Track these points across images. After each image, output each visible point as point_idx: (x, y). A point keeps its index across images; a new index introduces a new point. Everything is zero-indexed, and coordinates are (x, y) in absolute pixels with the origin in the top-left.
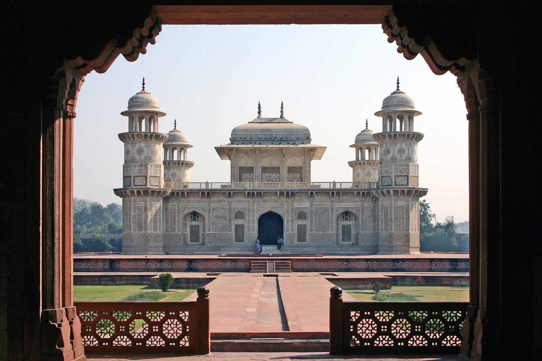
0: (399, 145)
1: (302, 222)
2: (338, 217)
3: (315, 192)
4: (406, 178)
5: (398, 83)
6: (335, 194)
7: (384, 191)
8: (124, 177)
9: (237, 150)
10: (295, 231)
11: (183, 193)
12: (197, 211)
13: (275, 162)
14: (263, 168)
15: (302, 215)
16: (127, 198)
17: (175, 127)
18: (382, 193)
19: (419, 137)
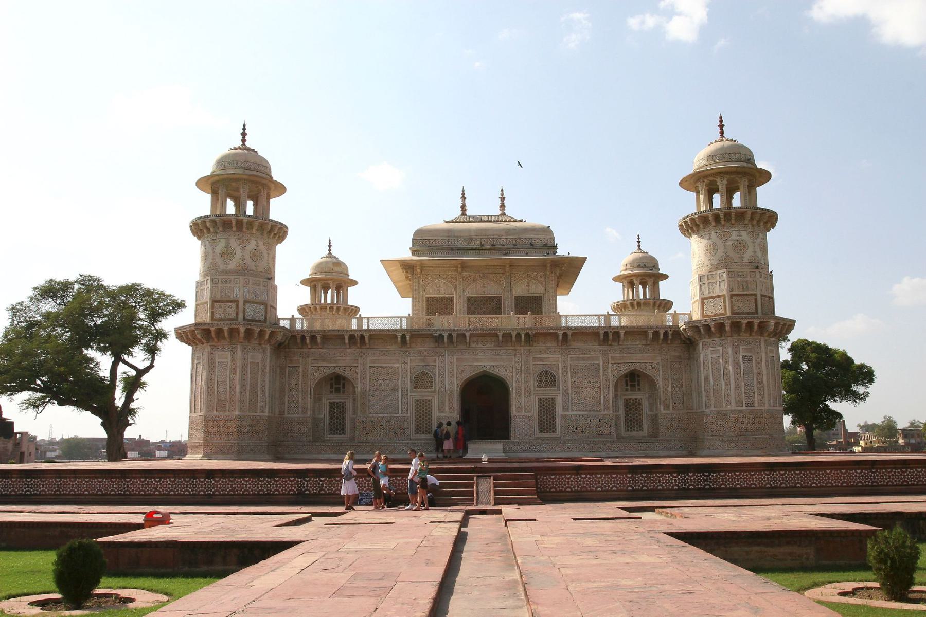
0: (734, 236)
1: (548, 393)
2: (616, 384)
3: (570, 337)
4: (753, 298)
5: (721, 126)
6: (611, 337)
7: (711, 324)
8: (197, 305)
9: (422, 264)
10: (534, 412)
11: (313, 338)
12: (340, 371)
13: (492, 290)
14: (469, 299)
15: (547, 379)
16: (200, 346)
17: (330, 250)
18: (707, 327)
19: (769, 219)
